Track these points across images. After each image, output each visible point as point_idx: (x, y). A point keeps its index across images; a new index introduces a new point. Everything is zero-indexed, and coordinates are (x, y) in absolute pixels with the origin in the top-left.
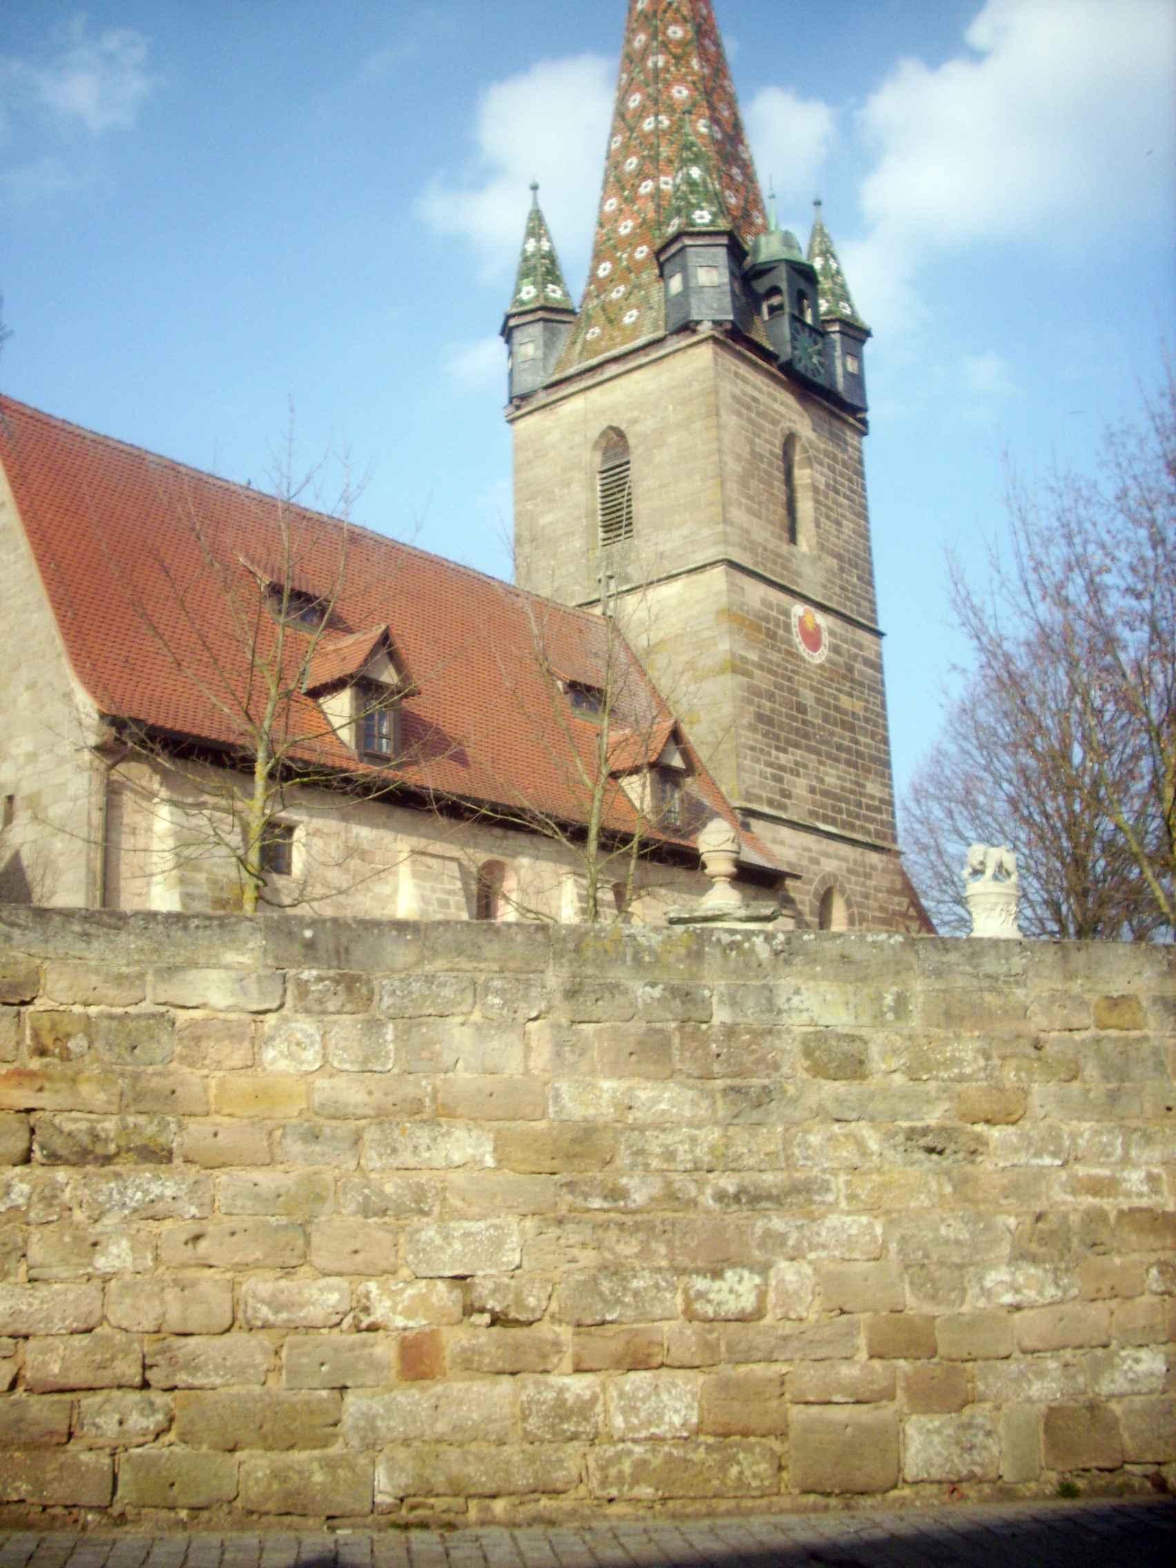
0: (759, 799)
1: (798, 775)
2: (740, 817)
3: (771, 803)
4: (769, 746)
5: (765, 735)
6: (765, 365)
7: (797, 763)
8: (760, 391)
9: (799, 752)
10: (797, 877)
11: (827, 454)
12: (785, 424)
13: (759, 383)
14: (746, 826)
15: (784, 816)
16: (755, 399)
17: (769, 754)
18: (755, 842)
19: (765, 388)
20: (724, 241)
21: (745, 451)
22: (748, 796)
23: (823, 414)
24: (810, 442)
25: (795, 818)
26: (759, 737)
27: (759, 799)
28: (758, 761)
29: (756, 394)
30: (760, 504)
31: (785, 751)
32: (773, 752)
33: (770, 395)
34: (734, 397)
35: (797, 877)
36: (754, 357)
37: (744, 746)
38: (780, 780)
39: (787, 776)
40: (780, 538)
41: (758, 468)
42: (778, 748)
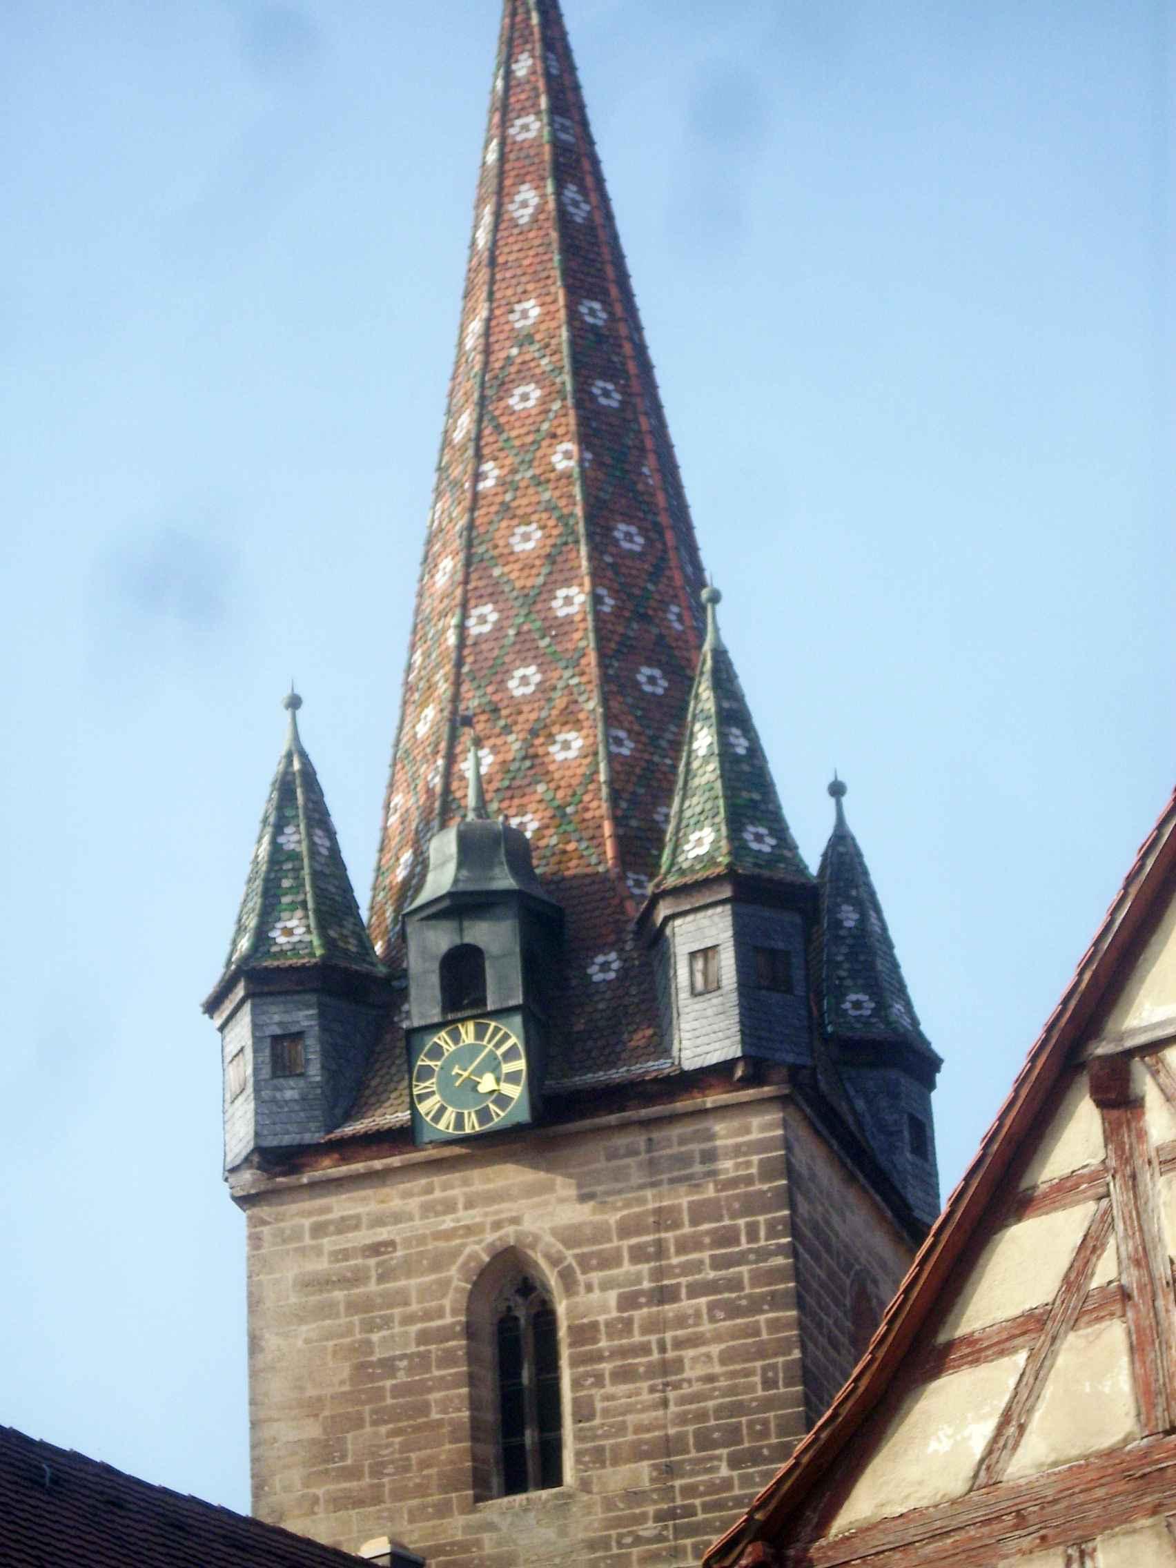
6: (396, 1161)
8: (397, 1218)
11: (625, 1230)
12: (478, 1249)
13: (396, 1204)
16: (376, 1249)
19: (414, 1204)
20: (240, 991)
21: (339, 1375)
23: (621, 1141)
24: (570, 1237)
29: (383, 1234)
30: (377, 1471)
33: (428, 1210)
34: (312, 1283)
36: (359, 1167)
40: (443, 1510)
41: (378, 1394)
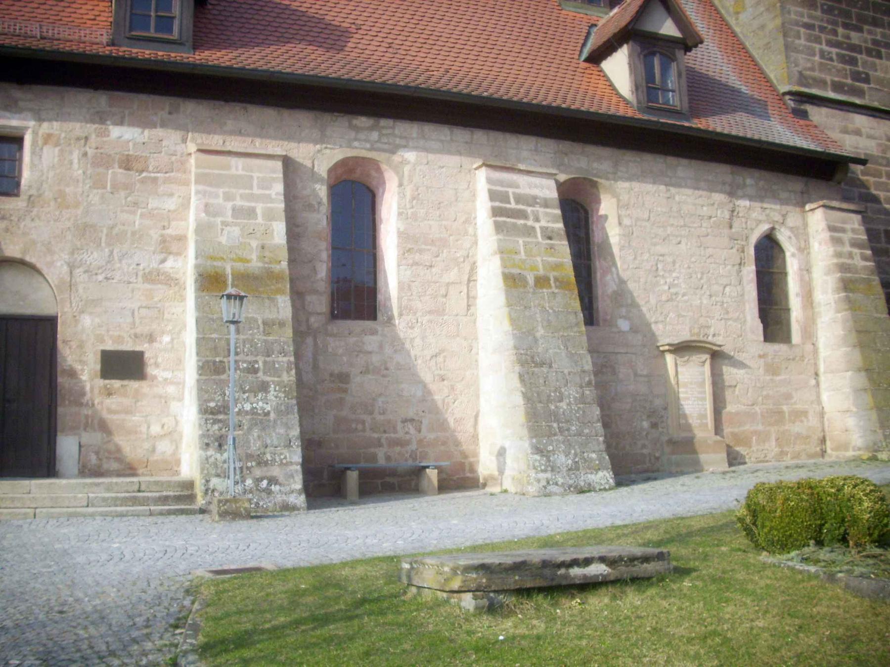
0: (822, 83)
1: (879, 56)
2: (792, 104)
3: (838, 87)
4: (834, 23)
5: (823, 11)
7: (875, 42)
9: (879, 30)
10: (863, 162)
14: (804, 115)
15: (858, 101)
17: (835, 33)
18: (811, 129)
22: (802, 79)
25: (876, 104)
26: (818, 13)
27: (822, 83)
28: (818, 40)
31: (859, 30)
32: (840, 30)
35: (863, 162)
37: (797, 24)
38: (853, 61)
39: (861, 57)
42: (846, 26)
